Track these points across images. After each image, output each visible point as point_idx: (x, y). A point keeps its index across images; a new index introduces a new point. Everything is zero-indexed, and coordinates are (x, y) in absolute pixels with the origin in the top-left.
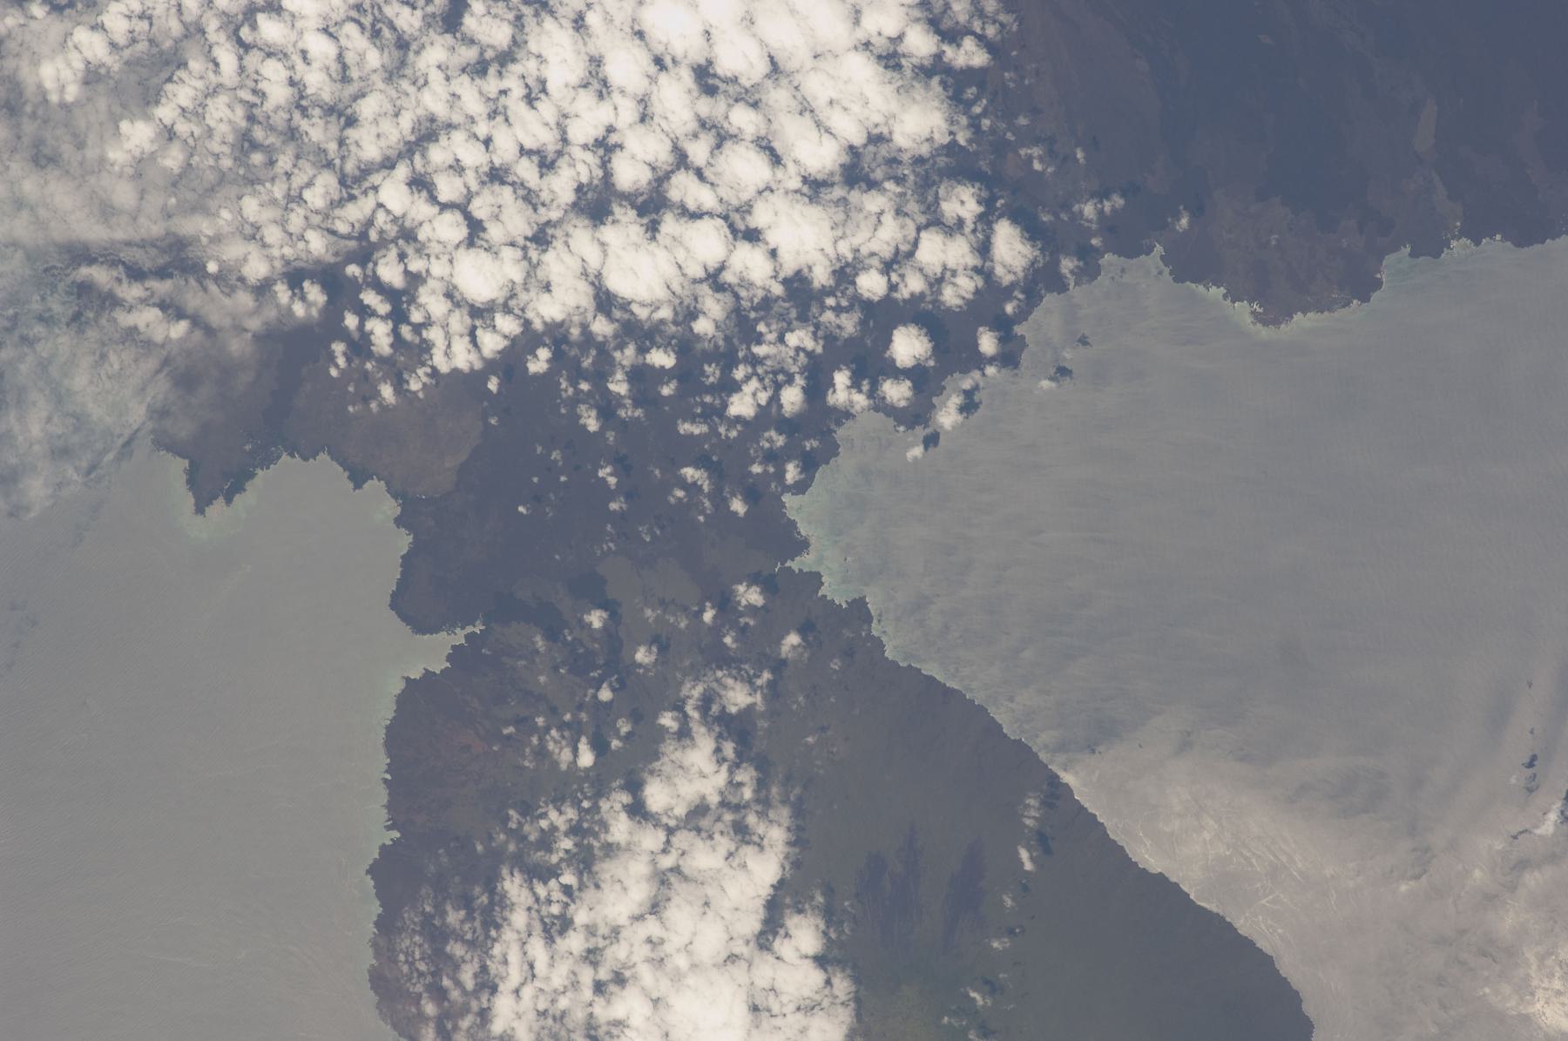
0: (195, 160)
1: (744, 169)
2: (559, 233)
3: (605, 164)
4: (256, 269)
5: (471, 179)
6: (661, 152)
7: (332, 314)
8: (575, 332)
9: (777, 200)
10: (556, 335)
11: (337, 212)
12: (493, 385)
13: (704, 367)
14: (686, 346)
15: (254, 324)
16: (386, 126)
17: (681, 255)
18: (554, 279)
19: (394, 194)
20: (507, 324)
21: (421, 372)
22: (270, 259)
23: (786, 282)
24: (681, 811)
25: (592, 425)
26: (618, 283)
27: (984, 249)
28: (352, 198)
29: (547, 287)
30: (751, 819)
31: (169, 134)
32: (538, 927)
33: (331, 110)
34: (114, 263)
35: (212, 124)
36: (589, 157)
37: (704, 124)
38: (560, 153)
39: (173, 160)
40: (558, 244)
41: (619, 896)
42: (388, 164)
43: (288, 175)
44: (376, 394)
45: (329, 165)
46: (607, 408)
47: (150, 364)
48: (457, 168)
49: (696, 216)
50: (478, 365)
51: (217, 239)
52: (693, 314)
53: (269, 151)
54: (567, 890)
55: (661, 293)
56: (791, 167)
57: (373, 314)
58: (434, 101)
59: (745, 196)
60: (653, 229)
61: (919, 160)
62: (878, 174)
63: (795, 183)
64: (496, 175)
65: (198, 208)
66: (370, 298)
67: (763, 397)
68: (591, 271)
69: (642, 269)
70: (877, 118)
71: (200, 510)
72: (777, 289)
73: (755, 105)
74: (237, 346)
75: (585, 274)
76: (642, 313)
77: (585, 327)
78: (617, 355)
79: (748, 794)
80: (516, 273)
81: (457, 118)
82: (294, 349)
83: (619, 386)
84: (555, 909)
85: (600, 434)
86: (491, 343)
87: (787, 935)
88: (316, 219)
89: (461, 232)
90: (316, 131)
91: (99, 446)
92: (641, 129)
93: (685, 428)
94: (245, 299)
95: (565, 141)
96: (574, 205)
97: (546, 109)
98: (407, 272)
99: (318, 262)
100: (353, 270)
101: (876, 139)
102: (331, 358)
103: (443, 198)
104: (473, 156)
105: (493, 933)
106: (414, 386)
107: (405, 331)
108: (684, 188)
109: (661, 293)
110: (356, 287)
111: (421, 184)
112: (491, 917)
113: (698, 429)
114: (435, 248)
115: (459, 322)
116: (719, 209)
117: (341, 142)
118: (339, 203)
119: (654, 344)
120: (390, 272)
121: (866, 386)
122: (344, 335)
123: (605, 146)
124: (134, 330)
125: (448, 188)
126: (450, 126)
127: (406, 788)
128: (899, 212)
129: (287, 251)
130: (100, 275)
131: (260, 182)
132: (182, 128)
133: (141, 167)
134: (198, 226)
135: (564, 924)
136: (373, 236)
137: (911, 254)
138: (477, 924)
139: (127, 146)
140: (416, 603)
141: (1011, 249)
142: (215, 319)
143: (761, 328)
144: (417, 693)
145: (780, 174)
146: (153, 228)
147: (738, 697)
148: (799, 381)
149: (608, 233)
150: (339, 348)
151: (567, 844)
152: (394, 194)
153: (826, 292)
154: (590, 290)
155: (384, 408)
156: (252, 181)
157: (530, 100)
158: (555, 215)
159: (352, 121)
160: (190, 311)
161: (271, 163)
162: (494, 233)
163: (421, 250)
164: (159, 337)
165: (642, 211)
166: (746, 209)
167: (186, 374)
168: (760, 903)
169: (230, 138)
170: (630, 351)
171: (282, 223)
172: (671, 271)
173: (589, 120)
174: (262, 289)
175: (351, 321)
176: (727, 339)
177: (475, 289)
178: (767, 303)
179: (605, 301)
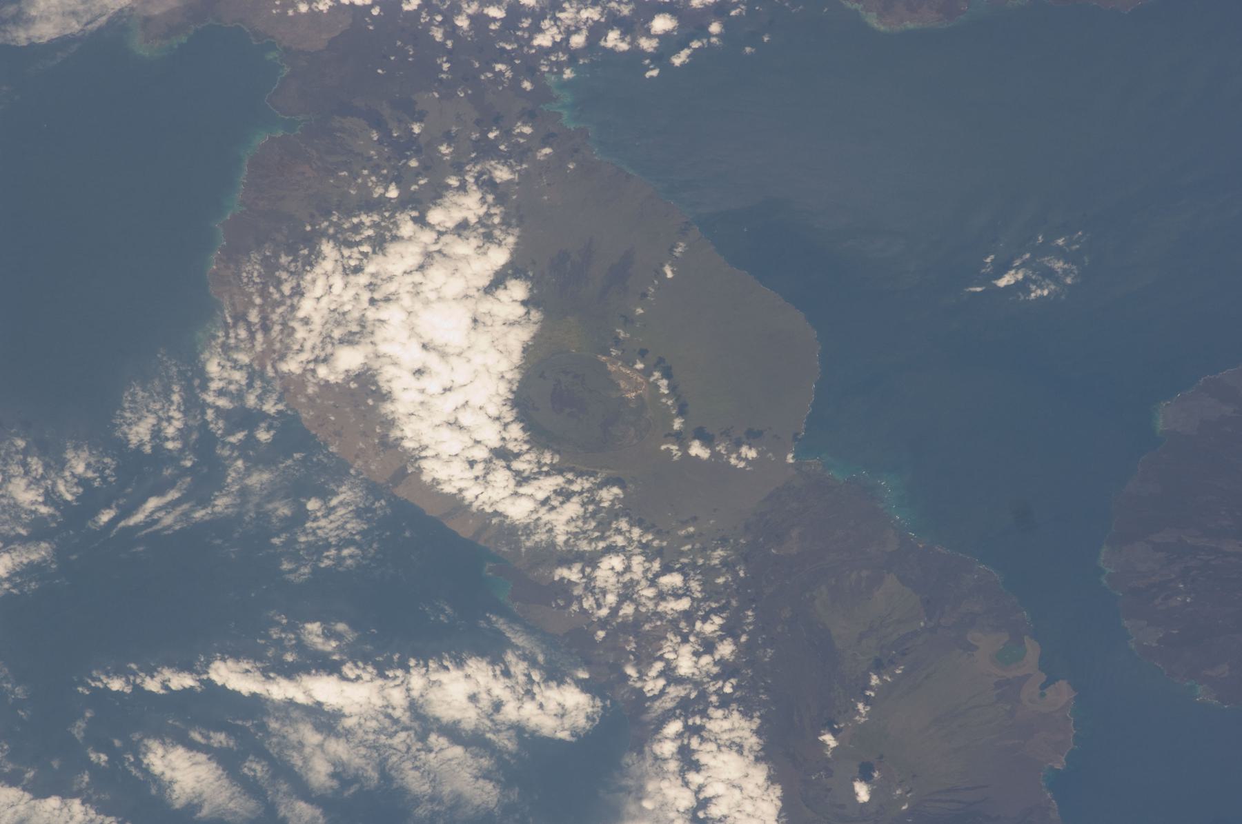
24: (451, 225)
30: (497, 233)
32: (340, 268)
41: (399, 260)
54: (365, 255)
79: (497, 220)
84: (353, 263)
87: (506, 288)
105: (308, 268)
112: (310, 262)
135: (358, 270)
138: (299, 264)
147: (502, 174)
151: (370, 232)
168: (491, 273)
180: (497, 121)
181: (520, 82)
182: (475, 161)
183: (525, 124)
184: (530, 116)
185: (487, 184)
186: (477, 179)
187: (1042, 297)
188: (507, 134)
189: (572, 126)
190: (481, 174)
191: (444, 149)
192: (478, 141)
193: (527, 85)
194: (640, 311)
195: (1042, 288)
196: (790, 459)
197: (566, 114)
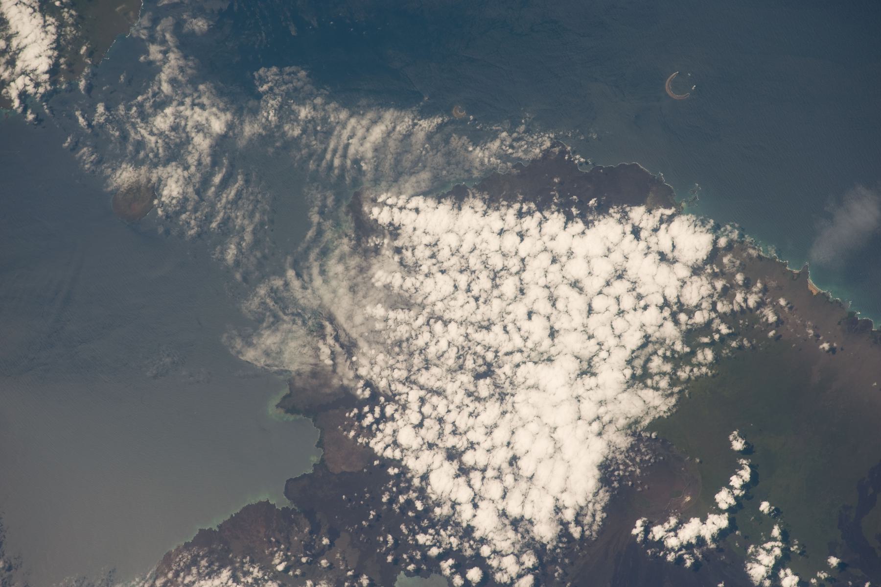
0: (383, 332)
1: (494, 490)
2: (436, 450)
3: (467, 449)
4: (363, 372)
5: (434, 414)
6: (481, 464)
7: (365, 402)
8: (409, 475)
9: (492, 506)
10: (405, 470)
11: (397, 383)
12: (376, 463)
13: (426, 519)
14: (428, 510)
15: (346, 382)
16: (433, 379)
17: (455, 490)
18: (421, 458)
19: (414, 395)
20: (397, 454)
21: (365, 439)
22: (369, 373)
23: (468, 526)
25: (385, 499)
26: (433, 478)
28: (404, 384)
29: (417, 458)
31: (386, 320)
33: (426, 360)
34: (335, 330)
35: (398, 329)
38: (460, 434)
39: (379, 326)
40: (433, 452)
42: (422, 388)
43: (398, 361)
44: (349, 431)
45: (409, 371)
46: (393, 500)
47: (312, 361)
48: (435, 408)
49: (470, 486)
50: (379, 454)
51: (364, 354)
52: (439, 505)
53: (401, 351)
55: (439, 492)
56: (504, 503)
57: (373, 414)
58: (450, 388)
59: (486, 496)
62: (520, 530)
63: (500, 508)
64: (441, 420)
65: (369, 343)
66: (377, 410)
68: (432, 467)
69: (443, 482)
70: (537, 518)
71: (277, 406)
72: (464, 525)
73: (516, 480)
74: (335, 382)
75: (429, 466)
76: (429, 490)
77: (413, 477)
78: (411, 492)
80: (415, 446)
81: (450, 398)
82: (347, 398)
83: (402, 499)
85: (383, 504)
86: (389, 453)
88: (390, 378)
89: (416, 422)
90: (417, 361)
91: (277, 363)
92: (485, 452)
93: (403, 527)
94: (351, 374)
95: (465, 433)
96: (448, 449)
97: (471, 421)
98: (393, 415)
99: (377, 388)
100: (382, 399)
101: (531, 522)
102: (351, 411)
103: (423, 410)
104: (442, 410)
106: (360, 440)
107: (375, 426)
108: (476, 477)
109: (439, 492)
110: (377, 403)
111: (422, 401)
113: (405, 531)
114: (406, 417)
115: (389, 440)
116: (477, 491)
117: (419, 370)
118: (401, 382)
119: (422, 500)
120: (389, 410)
122: (360, 409)
123: (472, 446)
124: (319, 349)
125: (427, 409)
126: (446, 397)
127: (235, 524)
129: (375, 377)
130: (329, 328)
131: (390, 355)
132: (390, 322)
133: (370, 318)
134: (364, 346)
136: (397, 398)
139: (374, 310)
140: (292, 487)
142: (339, 370)
143: (449, 528)
144: (267, 506)
145: (500, 501)
146: (354, 334)
149: (447, 464)
150: (356, 411)
152: (414, 395)
154: (425, 471)
155: (346, 437)
157: (471, 415)
158: (441, 445)
159: (427, 369)
160: (337, 361)
161: (398, 354)
162: (423, 432)
164: (322, 358)
165: (460, 469)
166: (482, 499)
167: (316, 373)
169: (397, 338)
170: (415, 495)
171: (382, 370)
172: (448, 490)
173: (476, 435)
174: (358, 377)
175: (366, 409)
176: (439, 520)
177: (401, 438)
178: (458, 524)
179: (425, 477)
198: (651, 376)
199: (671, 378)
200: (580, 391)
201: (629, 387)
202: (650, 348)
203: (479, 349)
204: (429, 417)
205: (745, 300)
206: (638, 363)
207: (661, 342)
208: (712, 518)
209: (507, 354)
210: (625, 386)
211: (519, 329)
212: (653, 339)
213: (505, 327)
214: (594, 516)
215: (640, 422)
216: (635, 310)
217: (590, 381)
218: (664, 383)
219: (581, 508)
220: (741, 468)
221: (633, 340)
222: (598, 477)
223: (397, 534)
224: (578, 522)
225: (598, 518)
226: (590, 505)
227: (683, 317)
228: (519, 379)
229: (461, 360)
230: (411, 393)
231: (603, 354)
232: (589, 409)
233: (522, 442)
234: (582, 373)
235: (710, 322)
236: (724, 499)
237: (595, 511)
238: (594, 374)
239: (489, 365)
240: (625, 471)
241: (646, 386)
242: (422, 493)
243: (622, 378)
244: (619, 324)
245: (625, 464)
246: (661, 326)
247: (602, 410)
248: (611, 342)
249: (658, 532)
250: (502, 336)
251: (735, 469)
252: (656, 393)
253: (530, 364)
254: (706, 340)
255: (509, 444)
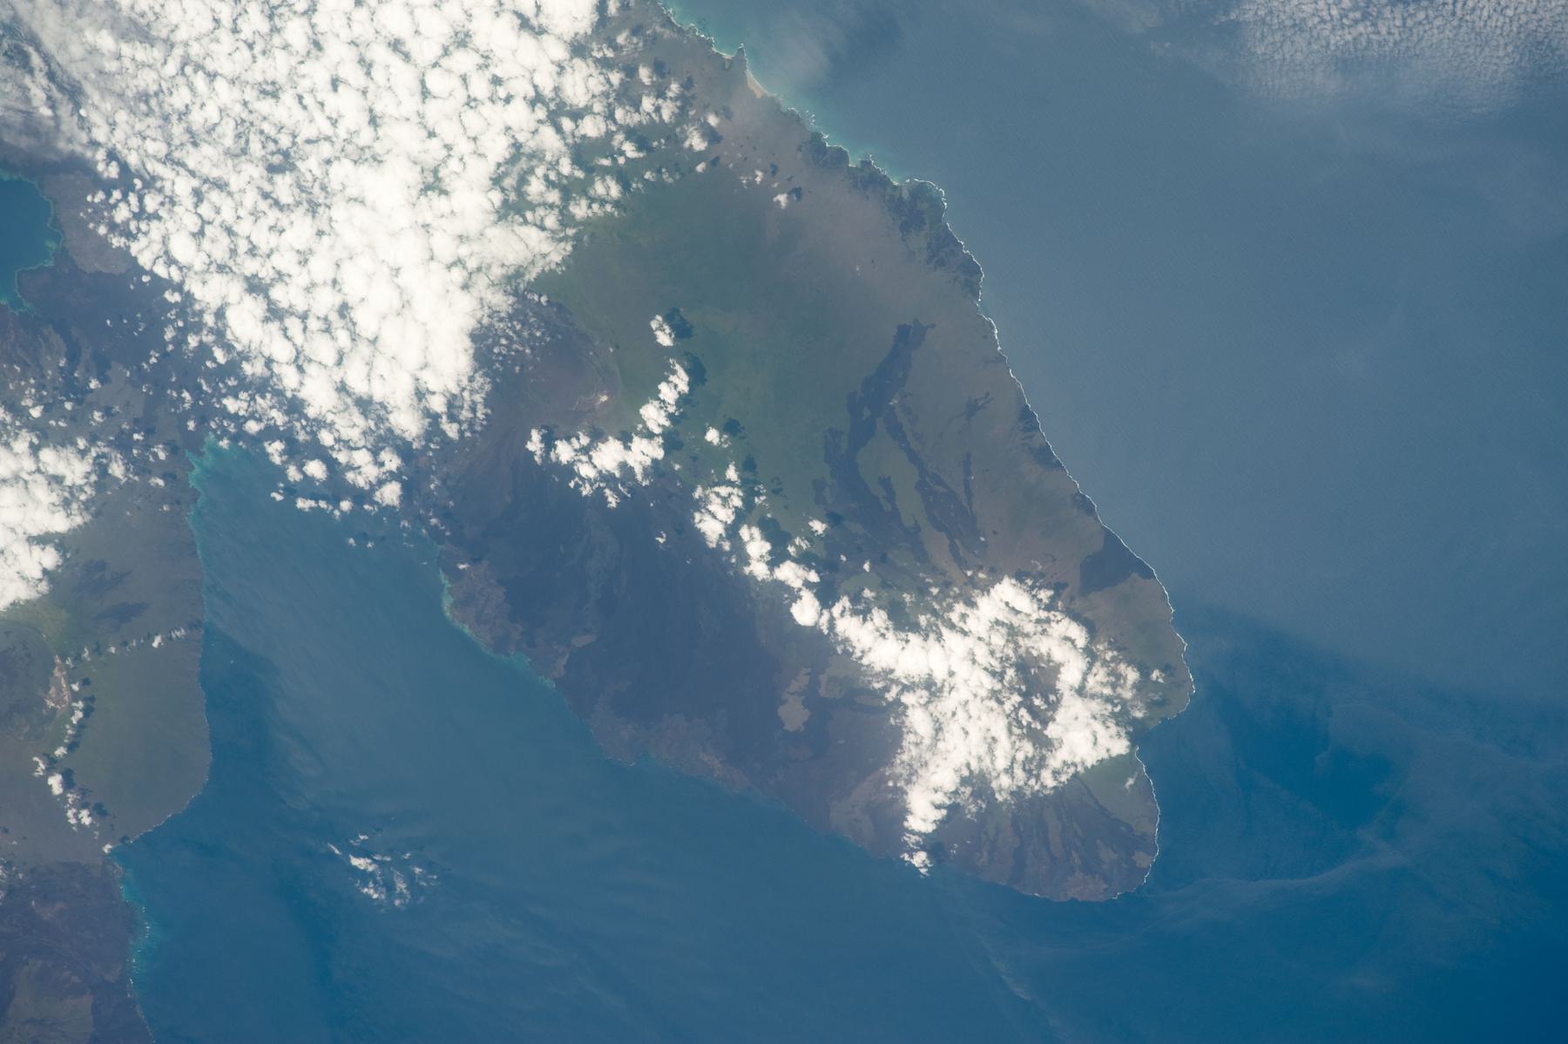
4: (100, 134)
5: (218, 221)
6: (301, 307)
10: (188, 298)
14: (232, 368)
17: (266, 341)
20: (175, 275)
26: (231, 315)
27: (381, 483)
29: (204, 283)
33: (189, 131)
36: (272, 274)
37: (326, 319)
42: (192, 173)
45: (169, 144)
46: (180, 341)
48: (218, 211)
51: (97, 108)
52: (247, 359)
58: (235, 183)
60: (266, 320)
61: (390, 431)
64: (230, 231)
67: (242, 413)
69: (246, 323)
72: (289, 394)
77: (201, 312)
86: (161, 270)
90: (177, 130)
95: (268, 256)
97: (273, 239)
100: (138, 183)
103: (200, 210)
109: (245, 341)
111: (198, 195)
118: (159, 160)
120: (151, 203)
121: (285, 458)
122: (109, 195)
123: (280, 276)
125: (205, 209)
128: (364, 433)
129: (119, 147)
136: (158, 184)
137: (352, 449)
141: (391, 494)
147: (117, 470)
148: (262, 426)
152: (183, 187)
153: (307, 419)
156: (132, 111)
163: (171, 211)
173: (286, 262)
174: (95, 144)
175: (117, 194)
179: (220, 314)
180: (149, 432)
181: (188, 419)
182: (109, 444)
183: (164, 449)
184: (173, 450)
185: (101, 468)
186: (98, 457)
187: (370, 897)
188: (146, 446)
189: (192, 484)
190: (104, 456)
191: (97, 415)
192: (122, 432)
193: (191, 425)
194: (113, 650)
195: (376, 891)
196: (107, 848)
197: (197, 470)
198: (532, 207)
199: (561, 212)
200: (429, 219)
201: (500, 219)
202: (523, 164)
203: (266, 127)
204: (209, 223)
205: (658, 109)
206: (509, 182)
207: (536, 155)
208: (638, 444)
209: (309, 141)
210: (493, 217)
211: (322, 104)
212: (526, 150)
213: (300, 98)
214: (473, 410)
215: (523, 275)
216: (492, 100)
217: (440, 203)
218: (551, 221)
219: (454, 396)
220: (674, 372)
221: (498, 149)
222: (471, 351)
223: (196, 391)
224: (453, 418)
225: (480, 415)
226: (466, 394)
227: (567, 124)
228: (334, 185)
229: (243, 141)
230: (178, 180)
231: (454, 164)
232: (445, 247)
233: (354, 285)
234: (426, 188)
235: (609, 135)
236: (653, 416)
237: (474, 403)
238: (444, 192)
239: (286, 154)
240: (508, 347)
241: (526, 222)
242: (220, 334)
243: (488, 206)
244: (470, 117)
245: (508, 338)
246: (535, 132)
247: (464, 251)
248: (463, 147)
249: (564, 452)
250: (298, 113)
251: (664, 374)
252: (543, 235)
253: (347, 164)
254: (606, 162)
255: (335, 282)
